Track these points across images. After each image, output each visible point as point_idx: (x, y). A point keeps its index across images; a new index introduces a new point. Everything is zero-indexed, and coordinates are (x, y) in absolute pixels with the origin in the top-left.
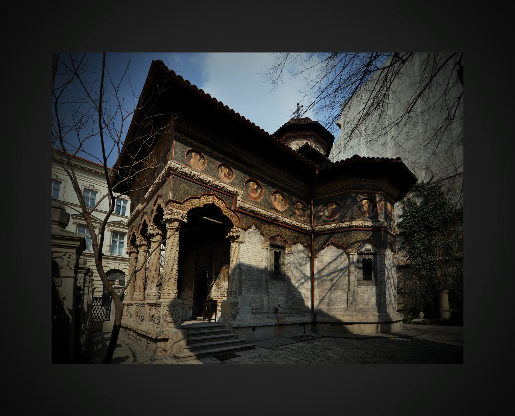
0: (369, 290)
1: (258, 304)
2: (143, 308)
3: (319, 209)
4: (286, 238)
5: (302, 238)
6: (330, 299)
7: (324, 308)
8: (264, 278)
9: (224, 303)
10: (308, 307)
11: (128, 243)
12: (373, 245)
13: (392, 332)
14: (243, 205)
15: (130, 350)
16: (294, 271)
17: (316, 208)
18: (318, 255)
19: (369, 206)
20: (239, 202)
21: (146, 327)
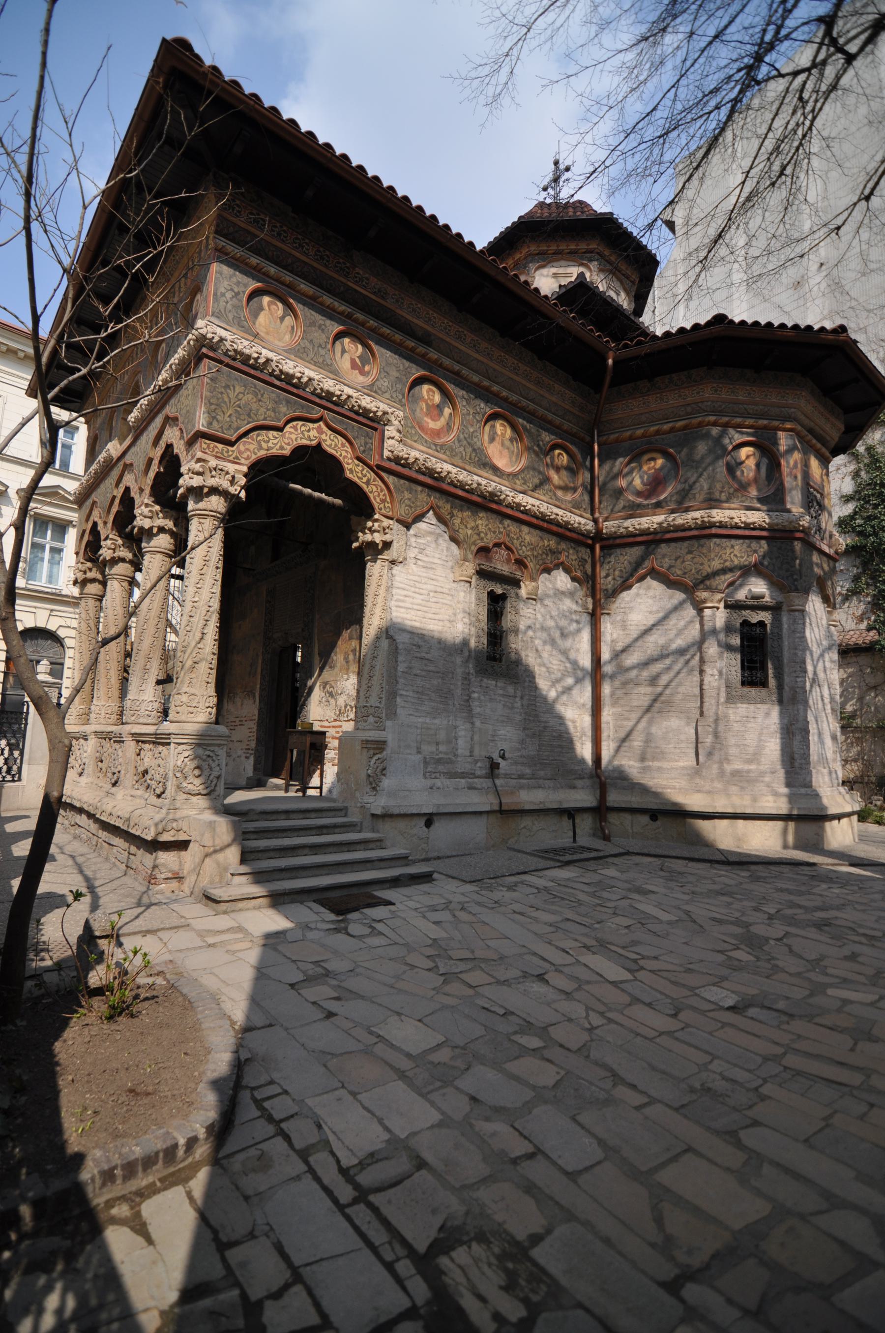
1: (442, 748)
2: (116, 746)
3: (616, 470)
4: (524, 551)
5: (570, 555)
7: (630, 764)
8: (460, 671)
9: (345, 741)
10: (583, 761)
11: (77, 553)
12: (773, 583)
13: (826, 848)
14: (402, 451)
15: (81, 872)
16: (546, 651)
17: (607, 467)
18: (614, 607)
19: (758, 465)
20: (391, 442)
21: (126, 805)
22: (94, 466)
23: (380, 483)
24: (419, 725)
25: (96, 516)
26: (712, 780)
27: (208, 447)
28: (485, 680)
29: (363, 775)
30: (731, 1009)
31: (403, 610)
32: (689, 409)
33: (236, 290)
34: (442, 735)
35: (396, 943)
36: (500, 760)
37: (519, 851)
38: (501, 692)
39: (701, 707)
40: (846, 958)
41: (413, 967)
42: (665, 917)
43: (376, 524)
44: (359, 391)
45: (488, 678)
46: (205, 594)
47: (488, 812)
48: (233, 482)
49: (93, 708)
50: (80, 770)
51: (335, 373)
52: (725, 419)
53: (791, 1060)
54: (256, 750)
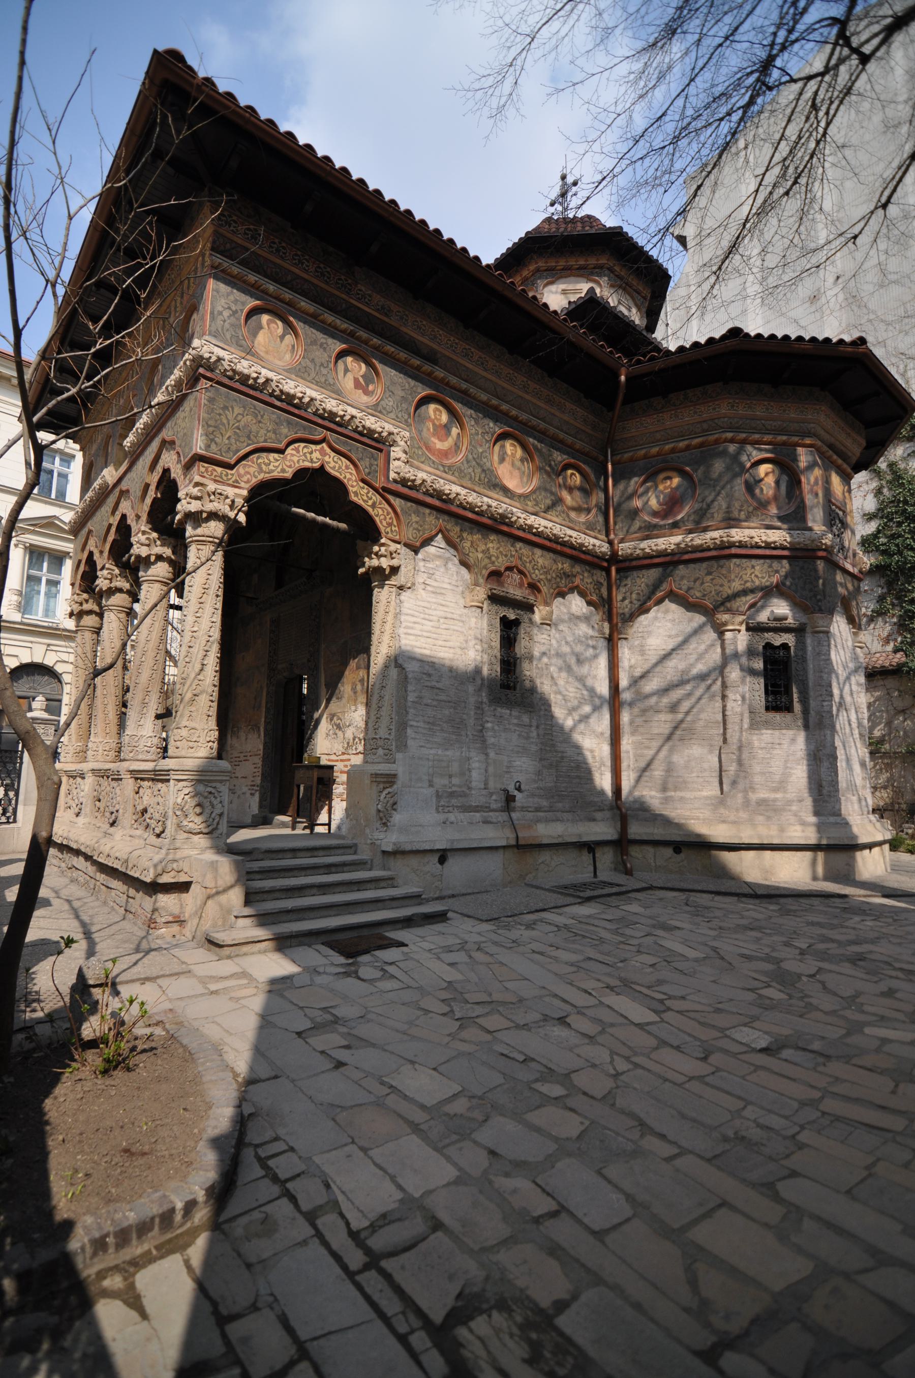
0: (786, 743)
1: (455, 781)
2: (114, 784)
3: (630, 489)
4: (537, 575)
5: (585, 579)
6: (670, 769)
7: (651, 795)
8: (472, 700)
9: (353, 774)
10: (602, 792)
11: (73, 585)
12: (795, 604)
13: (857, 878)
14: (409, 472)
15: (77, 917)
16: (562, 679)
17: (621, 486)
19: (777, 482)
20: (397, 463)
21: (124, 845)
22: (90, 494)
23: (387, 506)
24: (431, 757)
25: (91, 545)
26: (737, 810)
27: (207, 471)
28: (499, 709)
29: (373, 811)
30: (763, 1050)
31: (412, 637)
32: (705, 426)
33: (234, 308)
34: (455, 768)
35: (409, 987)
36: (516, 793)
37: (537, 887)
38: (515, 721)
39: (724, 734)
40: (883, 994)
41: (427, 1012)
42: (691, 954)
43: (383, 549)
44: (363, 411)
45: (502, 707)
46: (205, 623)
47: (504, 847)
48: (232, 506)
49: (90, 745)
50: (77, 810)
51: (338, 393)
52: (744, 435)
53: (829, 1105)
54: (262, 786)
